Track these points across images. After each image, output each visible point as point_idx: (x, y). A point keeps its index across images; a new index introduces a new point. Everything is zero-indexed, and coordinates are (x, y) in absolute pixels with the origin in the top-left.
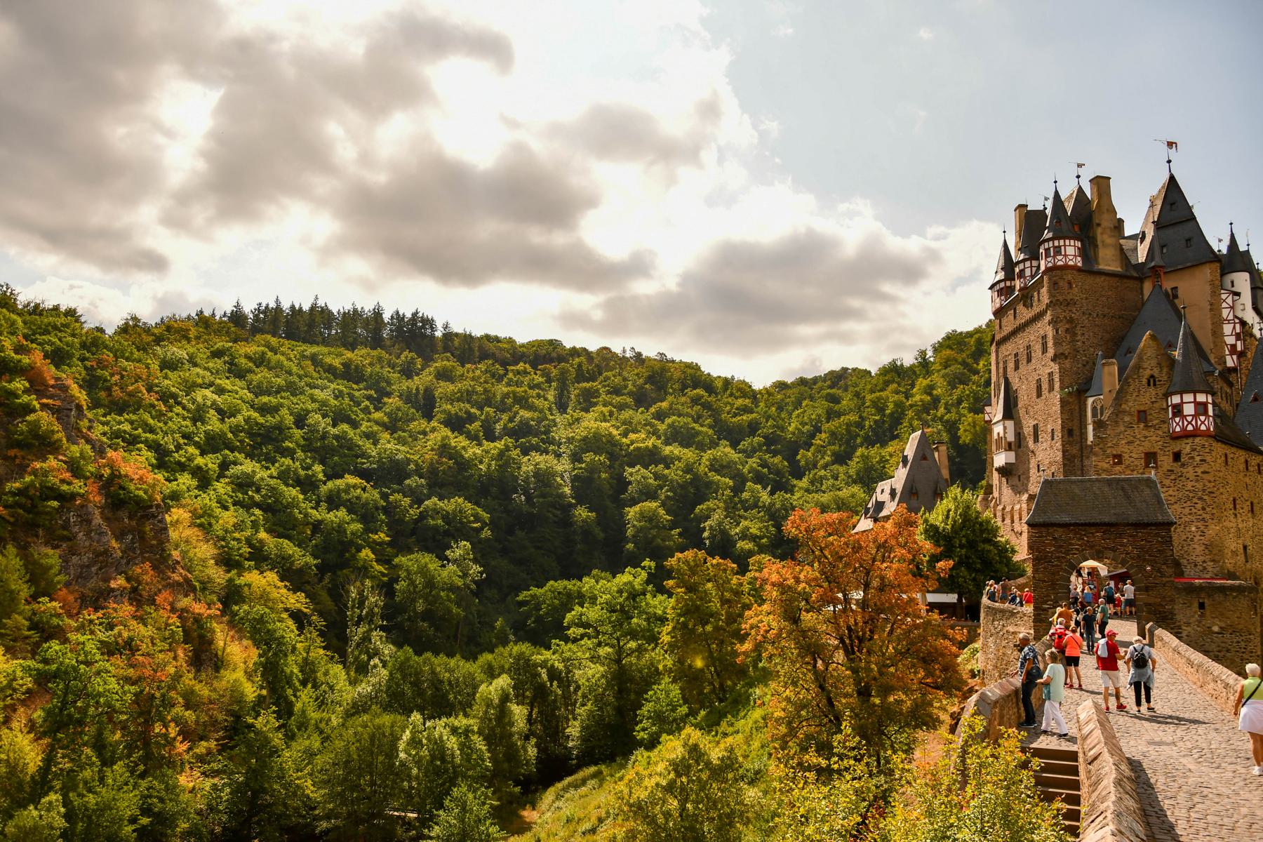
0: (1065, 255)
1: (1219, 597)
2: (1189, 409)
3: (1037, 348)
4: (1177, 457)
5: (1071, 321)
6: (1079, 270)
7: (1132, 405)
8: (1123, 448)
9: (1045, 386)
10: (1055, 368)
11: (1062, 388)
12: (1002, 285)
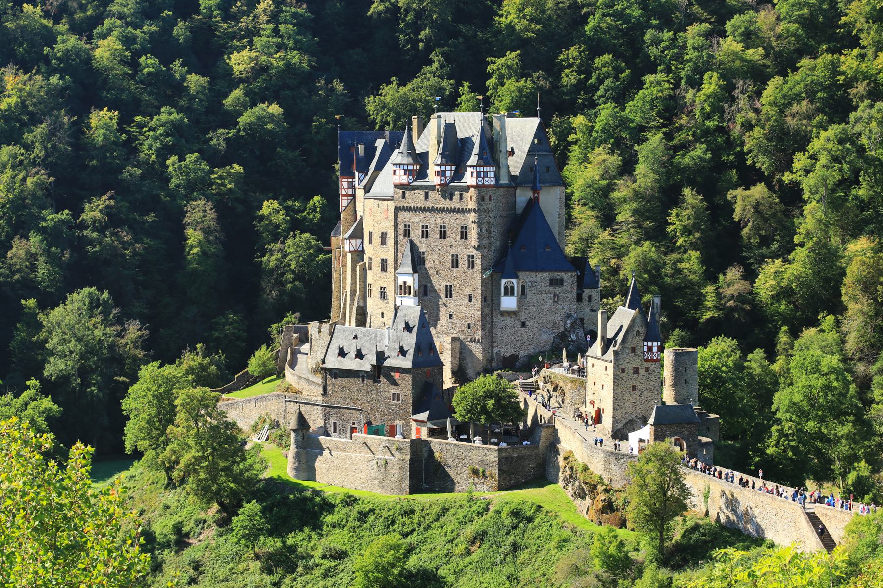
0: (490, 178)
1: (709, 447)
2: (655, 349)
3: (454, 235)
4: (647, 369)
5: (489, 223)
6: (494, 186)
7: (629, 345)
8: (625, 365)
9: (463, 262)
10: (478, 255)
11: (484, 270)
12: (410, 167)
